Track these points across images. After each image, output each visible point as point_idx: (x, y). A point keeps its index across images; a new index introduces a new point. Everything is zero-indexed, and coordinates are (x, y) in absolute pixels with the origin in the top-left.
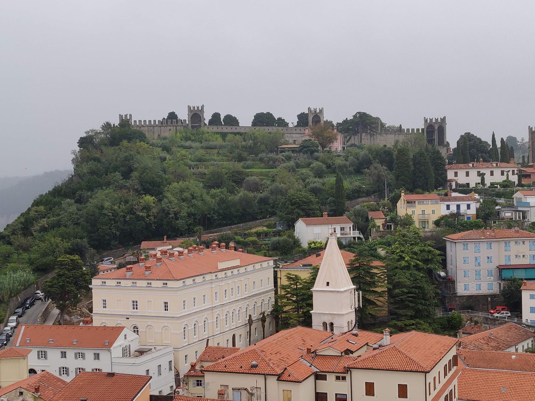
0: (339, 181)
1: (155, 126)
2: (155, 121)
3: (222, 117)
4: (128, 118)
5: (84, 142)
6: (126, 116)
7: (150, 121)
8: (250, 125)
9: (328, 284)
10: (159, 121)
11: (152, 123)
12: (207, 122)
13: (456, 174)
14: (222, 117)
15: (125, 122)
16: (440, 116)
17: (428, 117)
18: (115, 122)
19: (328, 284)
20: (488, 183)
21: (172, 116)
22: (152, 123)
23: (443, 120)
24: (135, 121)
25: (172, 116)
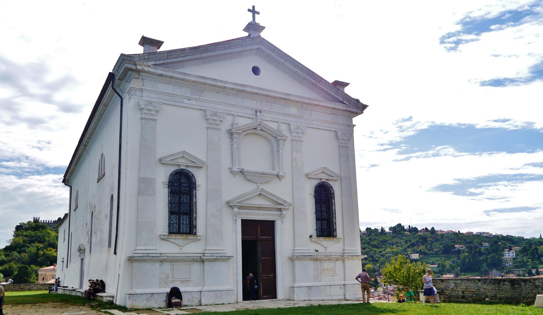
1: (51, 223)
2: (51, 221)
4: (38, 219)
6: (37, 218)
7: (49, 221)
10: (53, 221)
11: (50, 222)
15: (36, 221)
22: (50, 222)
24: (41, 221)
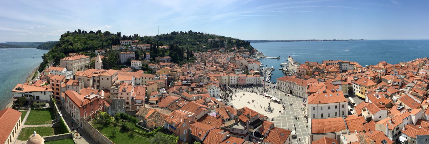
0: (102, 43)
3: (84, 31)
5: (62, 36)
8: (89, 33)
9: (98, 61)
12: (82, 32)
13: (122, 42)
14: (84, 31)
15: (68, 32)
16: (120, 32)
17: (118, 32)
18: (67, 32)
19: (98, 61)
20: (127, 44)
21: (76, 31)
23: (120, 32)
25: (76, 31)
